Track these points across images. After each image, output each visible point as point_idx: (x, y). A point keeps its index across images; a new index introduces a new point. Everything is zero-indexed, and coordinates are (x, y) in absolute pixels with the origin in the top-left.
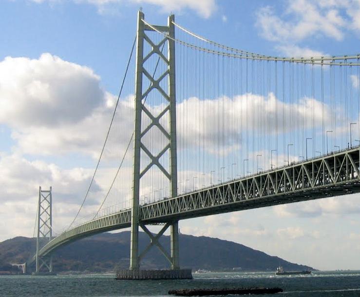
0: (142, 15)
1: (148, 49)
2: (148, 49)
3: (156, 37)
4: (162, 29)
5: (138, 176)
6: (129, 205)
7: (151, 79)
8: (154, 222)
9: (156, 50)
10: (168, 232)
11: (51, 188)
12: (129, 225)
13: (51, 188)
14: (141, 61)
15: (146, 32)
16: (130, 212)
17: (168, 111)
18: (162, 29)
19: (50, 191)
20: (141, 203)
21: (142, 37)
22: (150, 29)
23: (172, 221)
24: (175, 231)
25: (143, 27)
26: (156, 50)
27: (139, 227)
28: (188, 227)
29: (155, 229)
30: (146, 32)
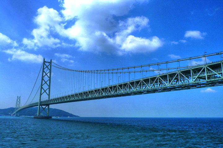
2: (45, 66)
4: (49, 62)
5: (41, 94)
6: (38, 101)
7: (45, 73)
8: (44, 105)
9: (47, 67)
10: (47, 107)
12: (38, 106)
18: (49, 62)
20: (41, 101)
23: (48, 105)
24: (48, 107)
26: (47, 67)
27: (41, 106)
28: (51, 106)
29: (44, 107)
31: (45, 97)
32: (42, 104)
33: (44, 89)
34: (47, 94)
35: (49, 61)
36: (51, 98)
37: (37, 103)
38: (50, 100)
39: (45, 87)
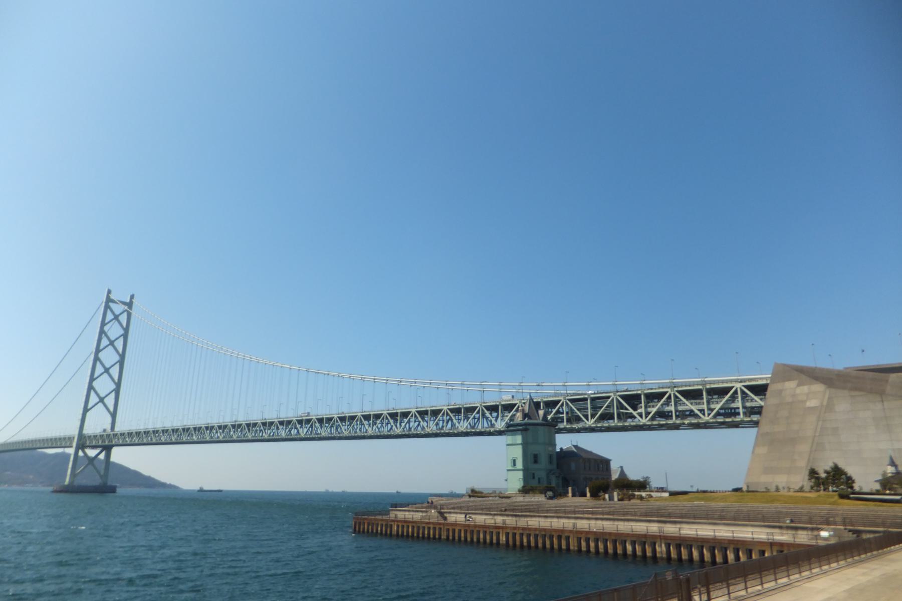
0: (109, 292)
1: (110, 316)
2: (110, 316)
3: (118, 308)
4: (124, 303)
5: (86, 410)
6: (75, 432)
9: (116, 317)
10: (102, 456)
12: (71, 447)
14: (103, 324)
15: (111, 304)
16: (74, 438)
17: (118, 363)
18: (124, 303)
20: (85, 432)
21: (107, 307)
22: (113, 301)
24: (108, 456)
25: (109, 300)
29: (92, 453)
30: (111, 304)
31: (98, 422)
32: (83, 442)
33: (99, 391)
34: (108, 409)
35: (128, 301)
36: (119, 428)
37: (71, 439)
38: (115, 435)
39: (104, 385)
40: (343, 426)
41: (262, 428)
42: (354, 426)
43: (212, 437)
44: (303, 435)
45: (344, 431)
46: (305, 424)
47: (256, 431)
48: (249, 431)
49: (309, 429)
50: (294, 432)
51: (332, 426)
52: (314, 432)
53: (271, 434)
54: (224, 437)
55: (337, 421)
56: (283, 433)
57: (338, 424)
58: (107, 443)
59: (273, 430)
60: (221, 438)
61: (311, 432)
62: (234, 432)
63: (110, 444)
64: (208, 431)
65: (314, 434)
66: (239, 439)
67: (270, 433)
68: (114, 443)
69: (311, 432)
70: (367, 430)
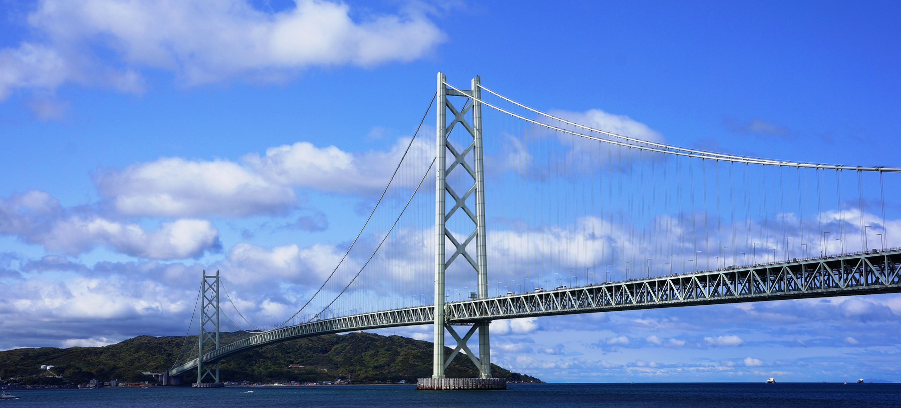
11: (218, 272)
13: (218, 272)
19: (217, 277)
23: (482, 324)
40: (797, 278)
41: (650, 289)
42: (815, 277)
43: (564, 307)
44: (737, 295)
45: (800, 287)
46: (710, 281)
47: (643, 293)
48: (632, 296)
49: (745, 285)
50: (722, 290)
51: (781, 279)
52: (753, 289)
53: (665, 297)
54: (580, 306)
55: (788, 272)
56: (707, 293)
57: (789, 276)
58: (478, 316)
59: (665, 291)
60: (576, 308)
61: (749, 289)
62: (592, 299)
63: (484, 316)
64: (559, 299)
65: (755, 293)
66: (850, 289)
67: (662, 296)
68: (490, 315)
69: (749, 289)
70: (837, 284)
